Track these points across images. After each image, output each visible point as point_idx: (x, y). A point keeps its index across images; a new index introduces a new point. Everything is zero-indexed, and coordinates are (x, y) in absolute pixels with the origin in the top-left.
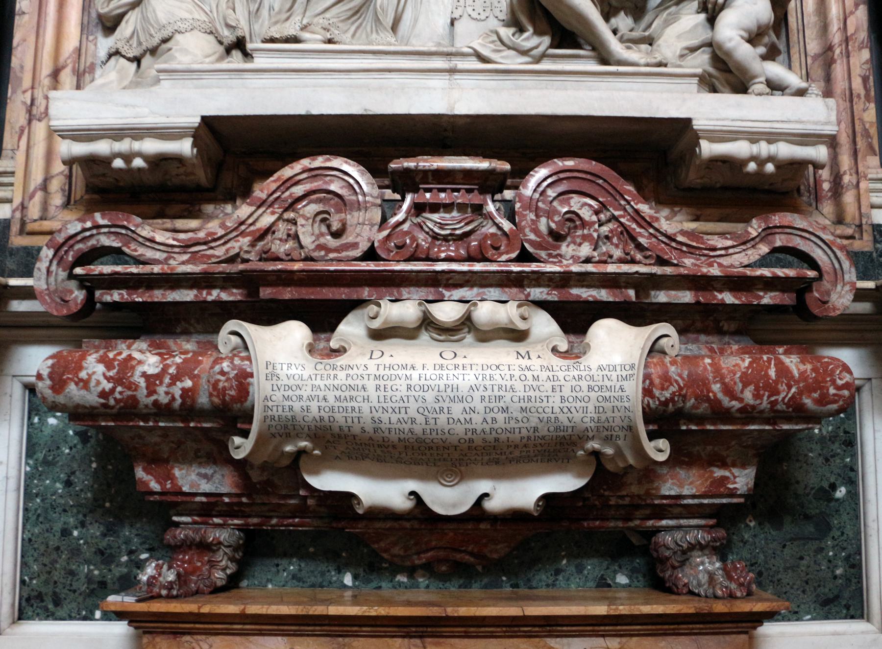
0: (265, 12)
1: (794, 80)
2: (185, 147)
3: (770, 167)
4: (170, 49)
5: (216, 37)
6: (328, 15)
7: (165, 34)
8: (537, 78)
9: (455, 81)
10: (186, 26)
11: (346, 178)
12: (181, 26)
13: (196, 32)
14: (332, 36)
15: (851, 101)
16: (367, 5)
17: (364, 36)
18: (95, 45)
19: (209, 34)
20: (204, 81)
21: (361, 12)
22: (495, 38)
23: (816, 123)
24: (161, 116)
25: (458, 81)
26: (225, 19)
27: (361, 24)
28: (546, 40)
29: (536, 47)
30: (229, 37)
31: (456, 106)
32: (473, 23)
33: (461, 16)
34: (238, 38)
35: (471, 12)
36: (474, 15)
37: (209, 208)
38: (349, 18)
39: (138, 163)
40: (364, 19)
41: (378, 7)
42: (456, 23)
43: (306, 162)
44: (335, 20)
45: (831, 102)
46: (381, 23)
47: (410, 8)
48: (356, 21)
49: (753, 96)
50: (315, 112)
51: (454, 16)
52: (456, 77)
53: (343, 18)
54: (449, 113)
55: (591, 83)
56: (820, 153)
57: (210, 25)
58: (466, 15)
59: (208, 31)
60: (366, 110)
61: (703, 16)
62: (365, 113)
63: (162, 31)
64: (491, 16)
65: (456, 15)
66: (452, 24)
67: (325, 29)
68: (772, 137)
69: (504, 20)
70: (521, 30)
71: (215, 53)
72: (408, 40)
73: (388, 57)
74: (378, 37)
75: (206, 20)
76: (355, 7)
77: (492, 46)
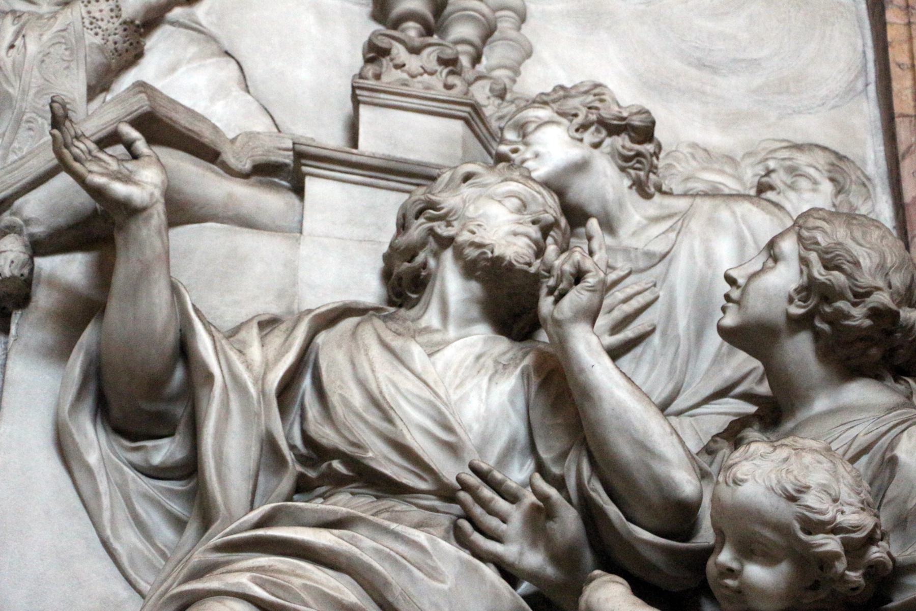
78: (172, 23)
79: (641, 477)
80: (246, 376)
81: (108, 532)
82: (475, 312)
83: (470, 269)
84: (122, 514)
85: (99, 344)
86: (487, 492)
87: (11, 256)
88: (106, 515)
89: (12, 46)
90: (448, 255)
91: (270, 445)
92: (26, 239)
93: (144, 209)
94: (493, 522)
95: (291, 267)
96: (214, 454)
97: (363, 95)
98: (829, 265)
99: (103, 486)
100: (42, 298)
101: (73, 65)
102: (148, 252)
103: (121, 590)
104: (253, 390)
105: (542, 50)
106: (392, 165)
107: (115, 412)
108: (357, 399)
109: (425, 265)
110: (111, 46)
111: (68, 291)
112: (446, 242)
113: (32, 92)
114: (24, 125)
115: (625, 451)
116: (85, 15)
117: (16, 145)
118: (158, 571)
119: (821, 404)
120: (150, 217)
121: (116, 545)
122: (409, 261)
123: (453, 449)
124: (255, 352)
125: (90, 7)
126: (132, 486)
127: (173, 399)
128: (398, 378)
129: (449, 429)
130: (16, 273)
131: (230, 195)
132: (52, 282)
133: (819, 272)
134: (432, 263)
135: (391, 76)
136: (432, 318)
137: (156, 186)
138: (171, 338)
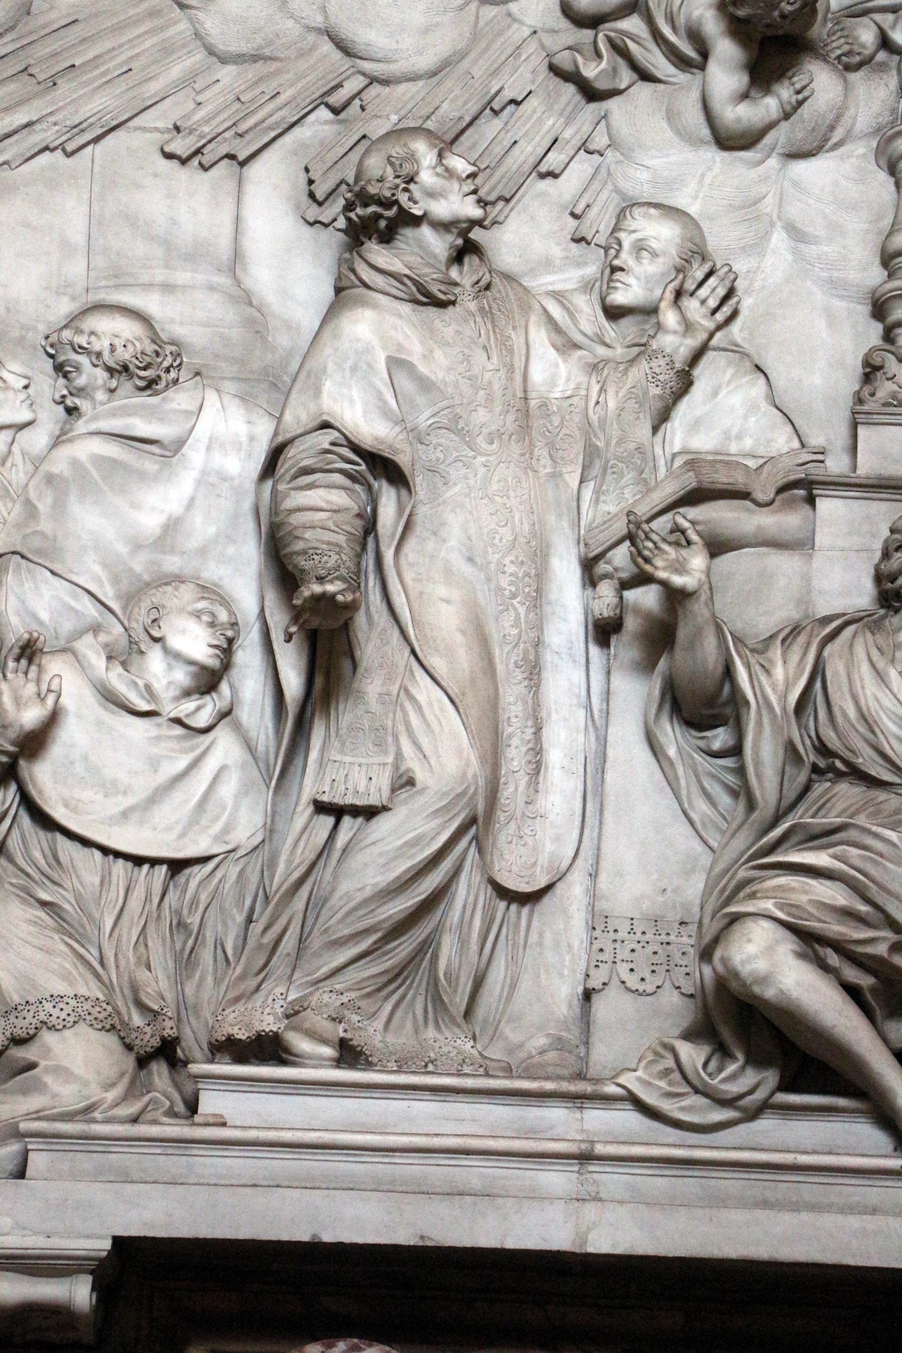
0: (206, 956)
4: (32, 1066)
5: (122, 1038)
6: (339, 983)
7: (22, 1025)
8: (746, 1176)
9: (589, 1176)
10: (63, 1015)
12: (52, 1011)
13: (82, 1028)
14: (348, 1036)
16: (418, 959)
17: (409, 1026)
19: (108, 1031)
20: (114, 1155)
21: (405, 974)
22: (670, 1063)
24: (35, 1233)
25: (595, 1176)
26: (135, 989)
27: (403, 997)
28: (771, 1077)
29: (751, 1092)
30: (149, 1040)
31: (590, 1236)
32: (630, 996)
33: (604, 984)
34: (163, 1039)
35: (625, 976)
36: (633, 981)
38: (379, 990)
40: (409, 987)
41: (441, 975)
42: (595, 998)
44: (353, 995)
46: (446, 1009)
47: (503, 963)
48: (394, 992)
50: (327, 1237)
51: (591, 984)
52: (592, 1168)
53: (368, 990)
54: (577, 1250)
55: (850, 1189)
57: (109, 1008)
58: (615, 981)
59: (108, 1026)
60: (422, 1237)
62: (421, 1243)
63: (12, 1018)
64: (667, 985)
65: (594, 983)
66: (588, 995)
67: (334, 1020)
69: (692, 996)
71: (122, 1075)
72: (496, 1029)
73: (460, 1097)
74: (439, 1036)
75: (102, 997)
76: (393, 968)
77: (662, 1084)
78: (714, 349)
80: (773, 699)
81: (686, 806)
84: (695, 789)
85: (670, 669)
87: (607, 601)
88: (684, 793)
89: (598, 403)
91: (792, 752)
92: (616, 581)
93: (695, 592)
95: (807, 579)
96: (753, 760)
97: (861, 418)
99: (680, 771)
100: (631, 624)
101: (641, 416)
102: (699, 619)
104: (778, 710)
106: (883, 482)
107: (685, 714)
108: (852, 713)
110: (668, 391)
111: (648, 616)
113: (614, 442)
114: (609, 471)
116: (648, 371)
117: (604, 488)
118: (723, 833)
120: (698, 598)
121: (693, 815)
122: (892, 582)
124: (779, 672)
125: (653, 364)
126: (700, 768)
127: (725, 704)
128: (880, 695)
130: (612, 614)
131: (759, 528)
132: (637, 610)
135: (885, 389)
138: (720, 670)
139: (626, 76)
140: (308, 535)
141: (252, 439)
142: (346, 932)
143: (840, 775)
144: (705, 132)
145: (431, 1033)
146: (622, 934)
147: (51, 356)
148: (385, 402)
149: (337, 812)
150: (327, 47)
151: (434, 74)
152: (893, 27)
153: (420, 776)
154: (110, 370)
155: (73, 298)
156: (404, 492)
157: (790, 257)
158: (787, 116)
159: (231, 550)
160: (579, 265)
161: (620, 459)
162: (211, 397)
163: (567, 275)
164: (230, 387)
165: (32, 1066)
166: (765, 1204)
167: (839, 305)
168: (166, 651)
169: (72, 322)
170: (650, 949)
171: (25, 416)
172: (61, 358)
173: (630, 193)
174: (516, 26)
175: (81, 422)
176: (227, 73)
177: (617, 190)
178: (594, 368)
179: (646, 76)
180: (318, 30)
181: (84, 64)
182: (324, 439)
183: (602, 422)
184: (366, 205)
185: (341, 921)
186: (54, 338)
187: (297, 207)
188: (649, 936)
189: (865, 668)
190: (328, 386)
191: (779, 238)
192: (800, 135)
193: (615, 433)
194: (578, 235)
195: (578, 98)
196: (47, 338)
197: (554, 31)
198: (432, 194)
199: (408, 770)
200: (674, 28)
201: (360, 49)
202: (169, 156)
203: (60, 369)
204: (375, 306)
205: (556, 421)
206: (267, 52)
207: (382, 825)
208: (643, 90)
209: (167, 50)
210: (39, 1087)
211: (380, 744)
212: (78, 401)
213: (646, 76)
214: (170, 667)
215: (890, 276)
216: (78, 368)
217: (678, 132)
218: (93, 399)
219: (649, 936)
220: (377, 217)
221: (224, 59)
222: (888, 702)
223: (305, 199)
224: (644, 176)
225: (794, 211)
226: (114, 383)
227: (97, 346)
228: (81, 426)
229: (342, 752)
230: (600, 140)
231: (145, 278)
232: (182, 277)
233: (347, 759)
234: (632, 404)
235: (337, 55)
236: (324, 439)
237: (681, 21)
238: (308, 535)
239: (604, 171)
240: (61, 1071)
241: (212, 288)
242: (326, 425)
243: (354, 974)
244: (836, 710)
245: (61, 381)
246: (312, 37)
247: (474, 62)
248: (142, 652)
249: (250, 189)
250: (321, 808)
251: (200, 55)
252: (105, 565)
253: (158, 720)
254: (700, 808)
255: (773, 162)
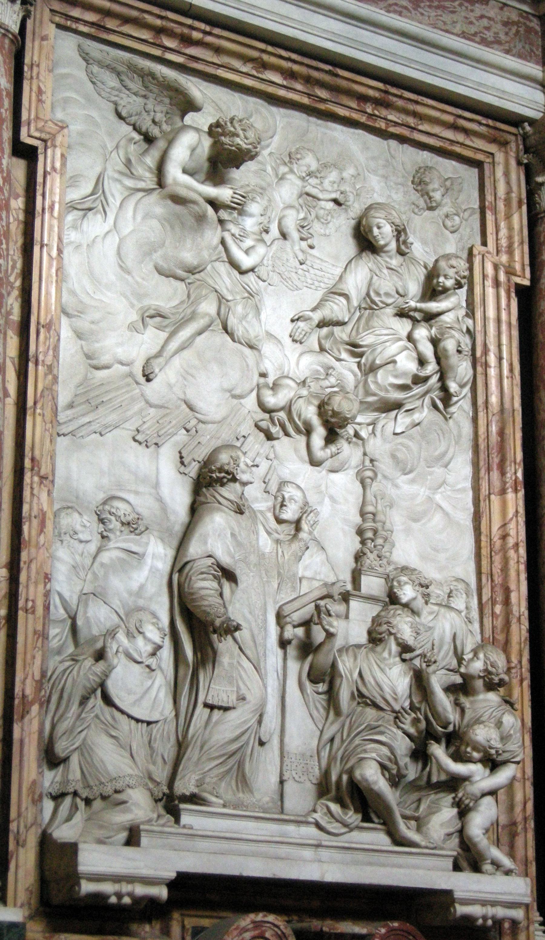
1: (507, 862)
2: (162, 893)
3: (490, 922)
7: (118, 786)
11: (276, 929)
15: (526, 865)
18: (43, 776)
23: (519, 895)
31: (326, 876)
35: (295, 775)
36: (297, 778)
37: (134, 927)
39: (127, 900)
43: (252, 916)
45: (528, 880)
49: (487, 876)
50: (245, 874)
56: (518, 914)
58: (291, 778)
61: (455, 811)
63: (114, 783)
68: (494, 904)
70: (343, 806)
73: (262, 821)
79: (442, 717)
82: (397, 655)
83: (398, 644)
86: (404, 713)
90: (392, 638)
94: (403, 720)
98: (492, 666)
103: (315, 728)
105: (397, 545)
109: (384, 637)
112: (391, 634)
115: (440, 709)
119: (481, 697)
123: (396, 700)
128: (383, 677)
129: (396, 694)
133: (490, 668)
134: (386, 637)
136: (386, 654)
137: (346, 638)
139: (281, 433)
140: (210, 599)
141: (166, 555)
142: (217, 754)
143: (367, 705)
144: (307, 458)
145: (241, 795)
146: (293, 760)
147: (98, 515)
148: (229, 549)
149: (212, 707)
150: (184, 406)
151: (219, 422)
152: (361, 430)
153: (248, 697)
154: (123, 524)
155: (104, 493)
156: (233, 585)
157: (330, 508)
158: (332, 457)
159: (159, 599)
160: (267, 501)
161: (288, 578)
162: (152, 539)
163: (262, 504)
164: (156, 533)
165: (124, 802)
166: (370, 864)
167: (346, 528)
168: (145, 638)
169: (104, 503)
170: (302, 765)
171: (89, 538)
172: (103, 516)
173: (283, 477)
174: (243, 408)
175: (111, 543)
176: (152, 411)
177: (278, 475)
178: (278, 542)
179: (287, 434)
180: (182, 400)
181: (107, 401)
182: (210, 561)
183: (283, 563)
184: (220, 472)
185: (215, 750)
186: (101, 508)
187: (176, 466)
188: (301, 761)
189: (375, 666)
190: (210, 541)
191: (327, 500)
192: (337, 465)
193: (286, 568)
194: (267, 490)
195: (265, 439)
196: (97, 507)
197: (255, 412)
198: (243, 472)
199: (243, 694)
200: (299, 419)
201: (197, 409)
202: (135, 440)
203: (102, 521)
204: (222, 511)
205: (267, 561)
206: (166, 405)
207: (231, 715)
208: (285, 439)
209: (133, 400)
210: (129, 810)
211: (231, 683)
212: (110, 535)
213: (287, 434)
214: (146, 644)
215: (364, 520)
216: (110, 521)
217: (298, 457)
218: (115, 534)
219: (301, 761)
220: (224, 477)
221: (151, 406)
222: (386, 680)
223: (179, 465)
224: (288, 471)
225: (332, 491)
226: (123, 529)
227: (119, 513)
228: (112, 545)
229: (215, 684)
230: (272, 456)
231: (129, 488)
232: (141, 489)
233: (217, 687)
234: (293, 558)
235: (188, 410)
236: (210, 561)
237: (303, 417)
238: (210, 599)
239: (273, 468)
240: (136, 804)
241: (150, 494)
242: (210, 556)
243: (216, 772)
244: (366, 681)
245: (101, 525)
246: (179, 402)
247: (232, 419)
248: (134, 637)
249: (161, 457)
250: (206, 705)
251: (143, 403)
252: (120, 601)
253: (143, 665)
254: (315, 713)
255: (324, 472)
